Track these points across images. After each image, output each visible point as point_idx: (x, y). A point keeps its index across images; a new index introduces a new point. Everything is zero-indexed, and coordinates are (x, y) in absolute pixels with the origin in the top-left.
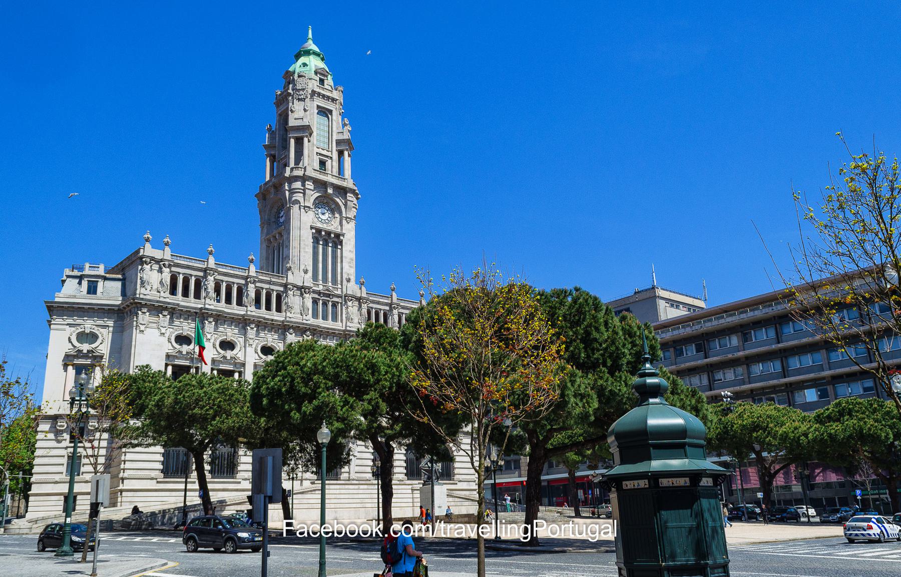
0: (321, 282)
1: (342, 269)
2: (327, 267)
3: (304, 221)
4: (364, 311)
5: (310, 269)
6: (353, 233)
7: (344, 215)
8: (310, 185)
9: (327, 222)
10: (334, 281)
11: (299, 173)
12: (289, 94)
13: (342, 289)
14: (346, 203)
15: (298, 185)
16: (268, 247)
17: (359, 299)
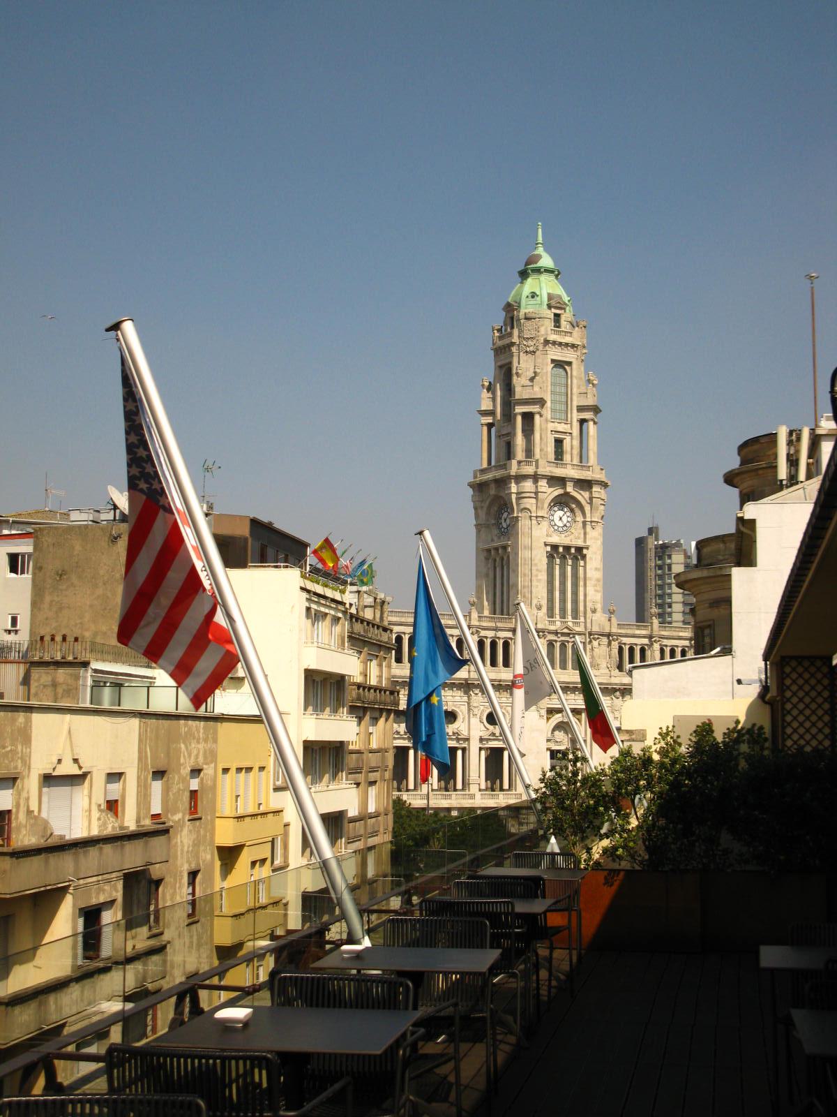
0: (558, 617)
1: (585, 595)
2: (564, 599)
3: (538, 531)
4: (615, 651)
5: (544, 602)
6: (599, 542)
7: (588, 519)
8: (543, 484)
9: (565, 529)
10: (575, 614)
11: (530, 470)
12: (513, 344)
13: (585, 622)
14: (591, 498)
15: (528, 485)
16: (487, 559)
17: (608, 635)
